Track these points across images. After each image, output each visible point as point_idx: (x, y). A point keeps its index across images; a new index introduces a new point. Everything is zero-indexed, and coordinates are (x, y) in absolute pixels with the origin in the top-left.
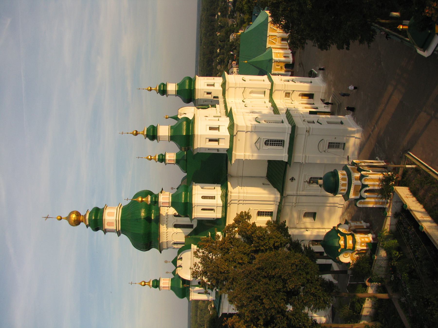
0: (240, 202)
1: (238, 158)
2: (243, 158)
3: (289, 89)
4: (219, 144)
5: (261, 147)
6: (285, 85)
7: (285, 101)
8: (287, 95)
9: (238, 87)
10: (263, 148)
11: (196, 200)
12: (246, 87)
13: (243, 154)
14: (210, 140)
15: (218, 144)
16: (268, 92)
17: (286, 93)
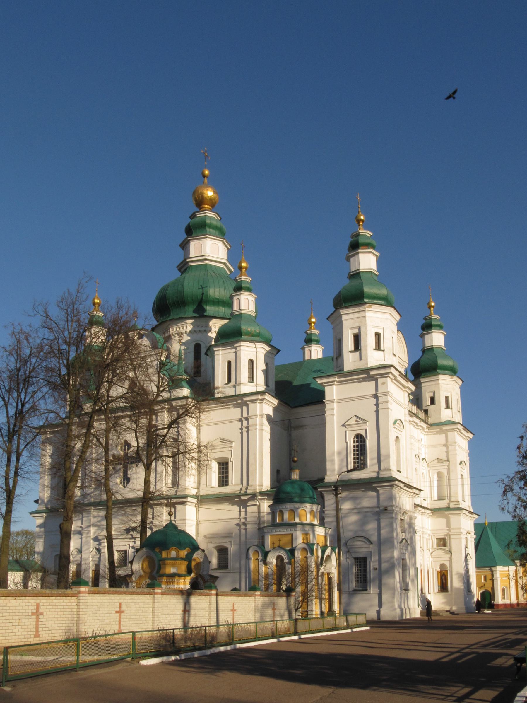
0: (245, 422)
1: (327, 389)
2: (327, 397)
3: (454, 544)
4: (351, 352)
5: (349, 429)
6: (460, 534)
7: (429, 539)
8: (442, 543)
9: (448, 449)
10: (347, 432)
11: (246, 348)
12: (449, 463)
13: (335, 398)
14: (357, 338)
15: (350, 350)
16: (443, 504)
17: (446, 538)
